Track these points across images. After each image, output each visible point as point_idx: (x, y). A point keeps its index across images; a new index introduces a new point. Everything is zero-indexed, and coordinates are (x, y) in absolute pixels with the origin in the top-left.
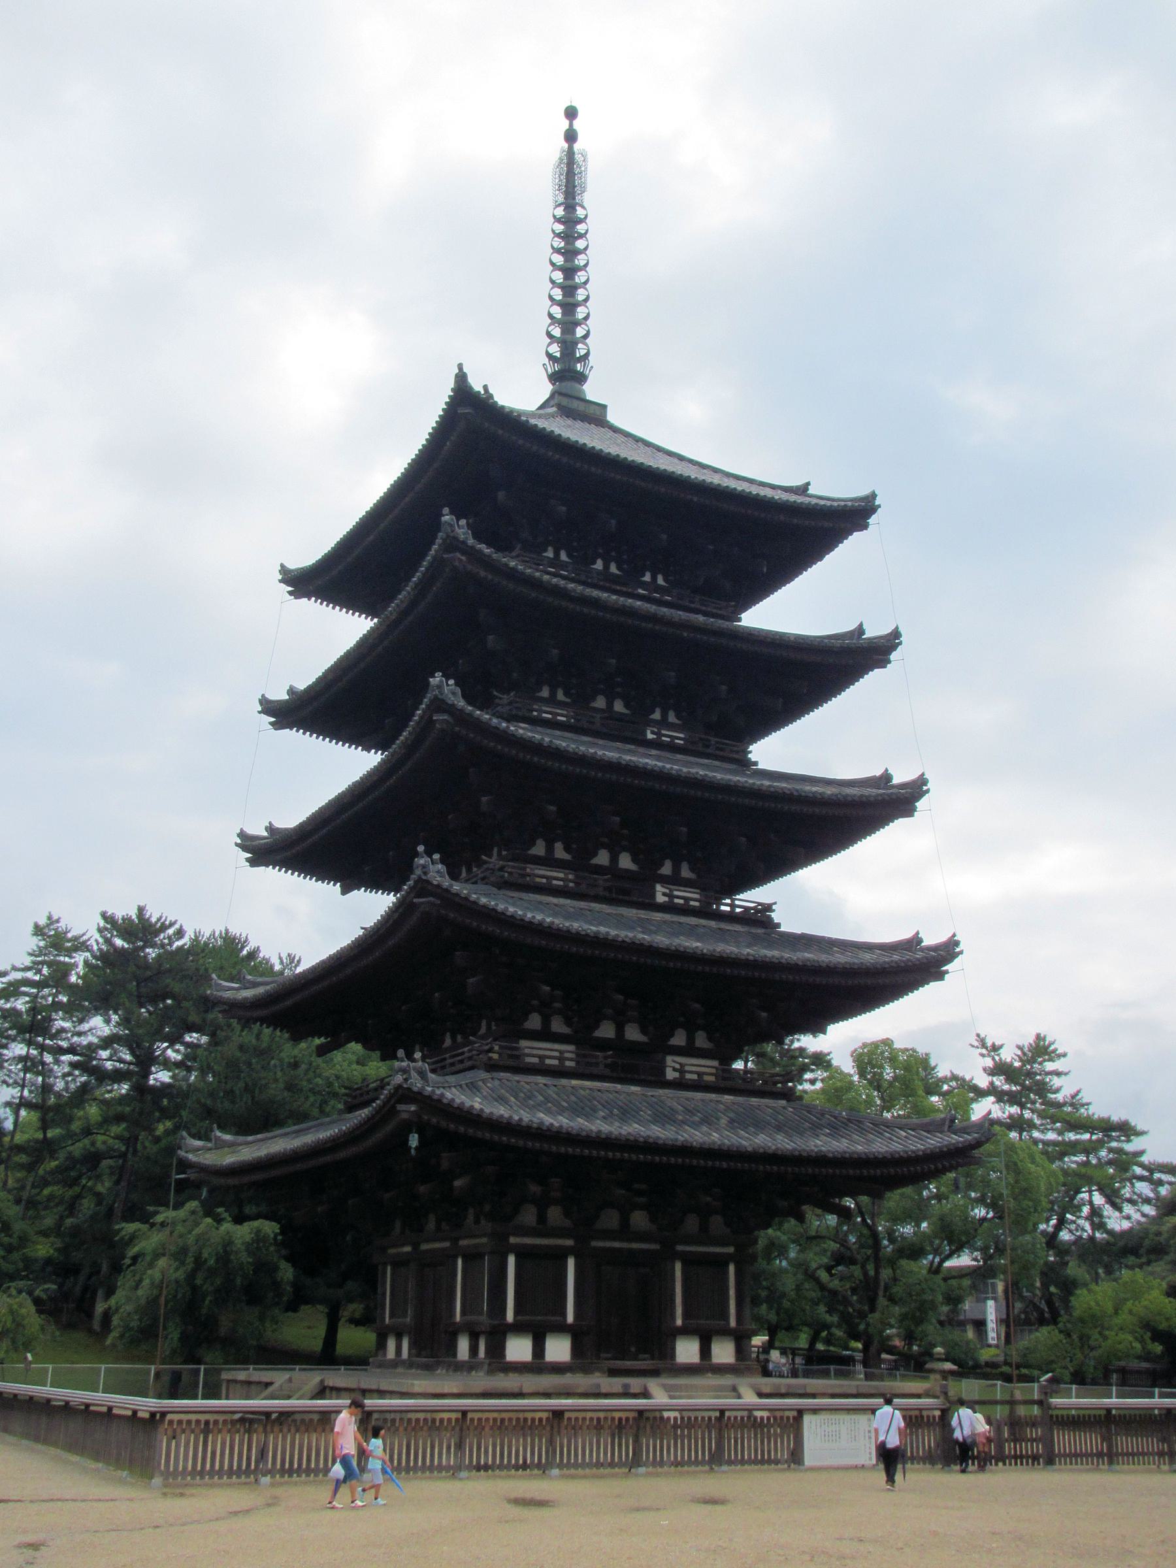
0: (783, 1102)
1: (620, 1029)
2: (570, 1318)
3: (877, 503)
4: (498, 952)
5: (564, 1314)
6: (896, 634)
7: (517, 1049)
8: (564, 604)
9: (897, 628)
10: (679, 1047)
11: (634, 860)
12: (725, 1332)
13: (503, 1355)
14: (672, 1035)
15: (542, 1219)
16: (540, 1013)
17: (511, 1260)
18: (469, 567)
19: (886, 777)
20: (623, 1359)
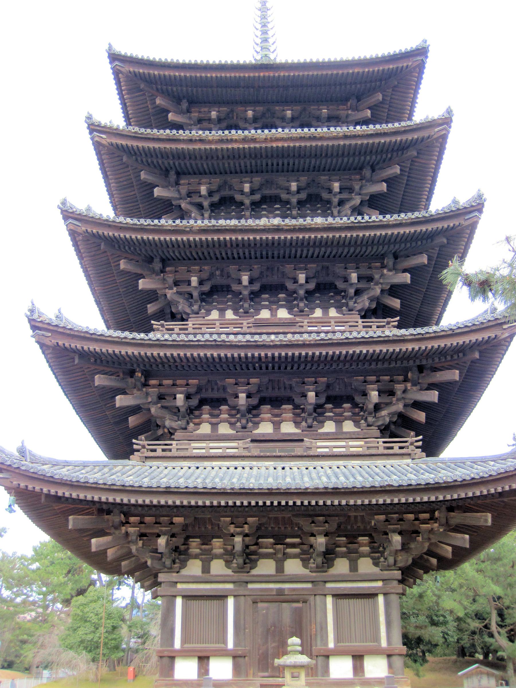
0: (409, 461)
1: (277, 425)
2: (230, 645)
3: (427, 44)
4: (140, 375)
5: (225, 642)
6: (449, 111)
7: (171, 445)
8: (180, 146)
9: (449, 107)
10: (328, 434)
11: (289, 313)
12: (376, 652)
13: (173, 675)
14: (323, 426)
15: (206, 569)
16: (212, 424)
17: (179, 601)
18: (109, 140)
19: (455, 202)
20: (279, 677)
